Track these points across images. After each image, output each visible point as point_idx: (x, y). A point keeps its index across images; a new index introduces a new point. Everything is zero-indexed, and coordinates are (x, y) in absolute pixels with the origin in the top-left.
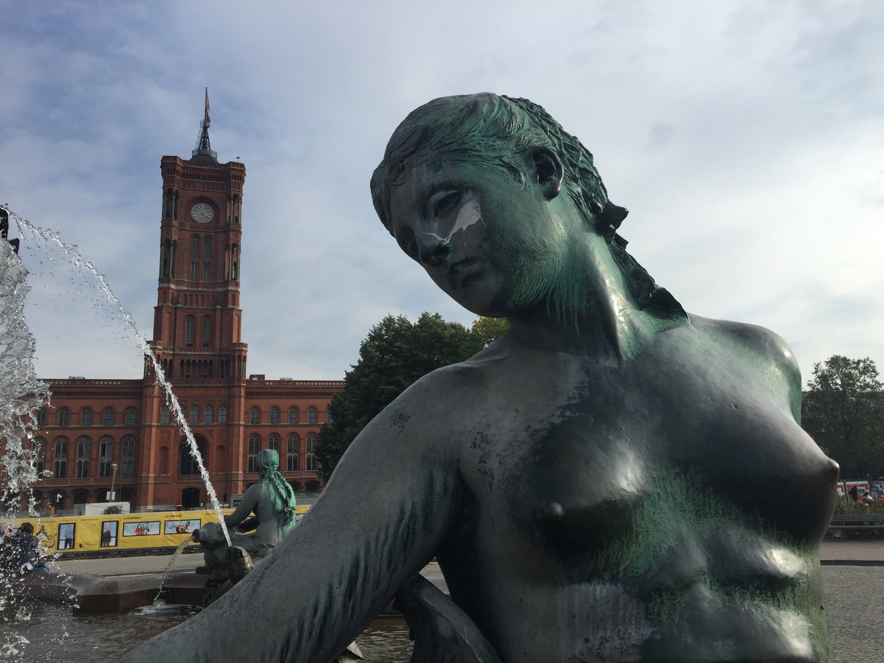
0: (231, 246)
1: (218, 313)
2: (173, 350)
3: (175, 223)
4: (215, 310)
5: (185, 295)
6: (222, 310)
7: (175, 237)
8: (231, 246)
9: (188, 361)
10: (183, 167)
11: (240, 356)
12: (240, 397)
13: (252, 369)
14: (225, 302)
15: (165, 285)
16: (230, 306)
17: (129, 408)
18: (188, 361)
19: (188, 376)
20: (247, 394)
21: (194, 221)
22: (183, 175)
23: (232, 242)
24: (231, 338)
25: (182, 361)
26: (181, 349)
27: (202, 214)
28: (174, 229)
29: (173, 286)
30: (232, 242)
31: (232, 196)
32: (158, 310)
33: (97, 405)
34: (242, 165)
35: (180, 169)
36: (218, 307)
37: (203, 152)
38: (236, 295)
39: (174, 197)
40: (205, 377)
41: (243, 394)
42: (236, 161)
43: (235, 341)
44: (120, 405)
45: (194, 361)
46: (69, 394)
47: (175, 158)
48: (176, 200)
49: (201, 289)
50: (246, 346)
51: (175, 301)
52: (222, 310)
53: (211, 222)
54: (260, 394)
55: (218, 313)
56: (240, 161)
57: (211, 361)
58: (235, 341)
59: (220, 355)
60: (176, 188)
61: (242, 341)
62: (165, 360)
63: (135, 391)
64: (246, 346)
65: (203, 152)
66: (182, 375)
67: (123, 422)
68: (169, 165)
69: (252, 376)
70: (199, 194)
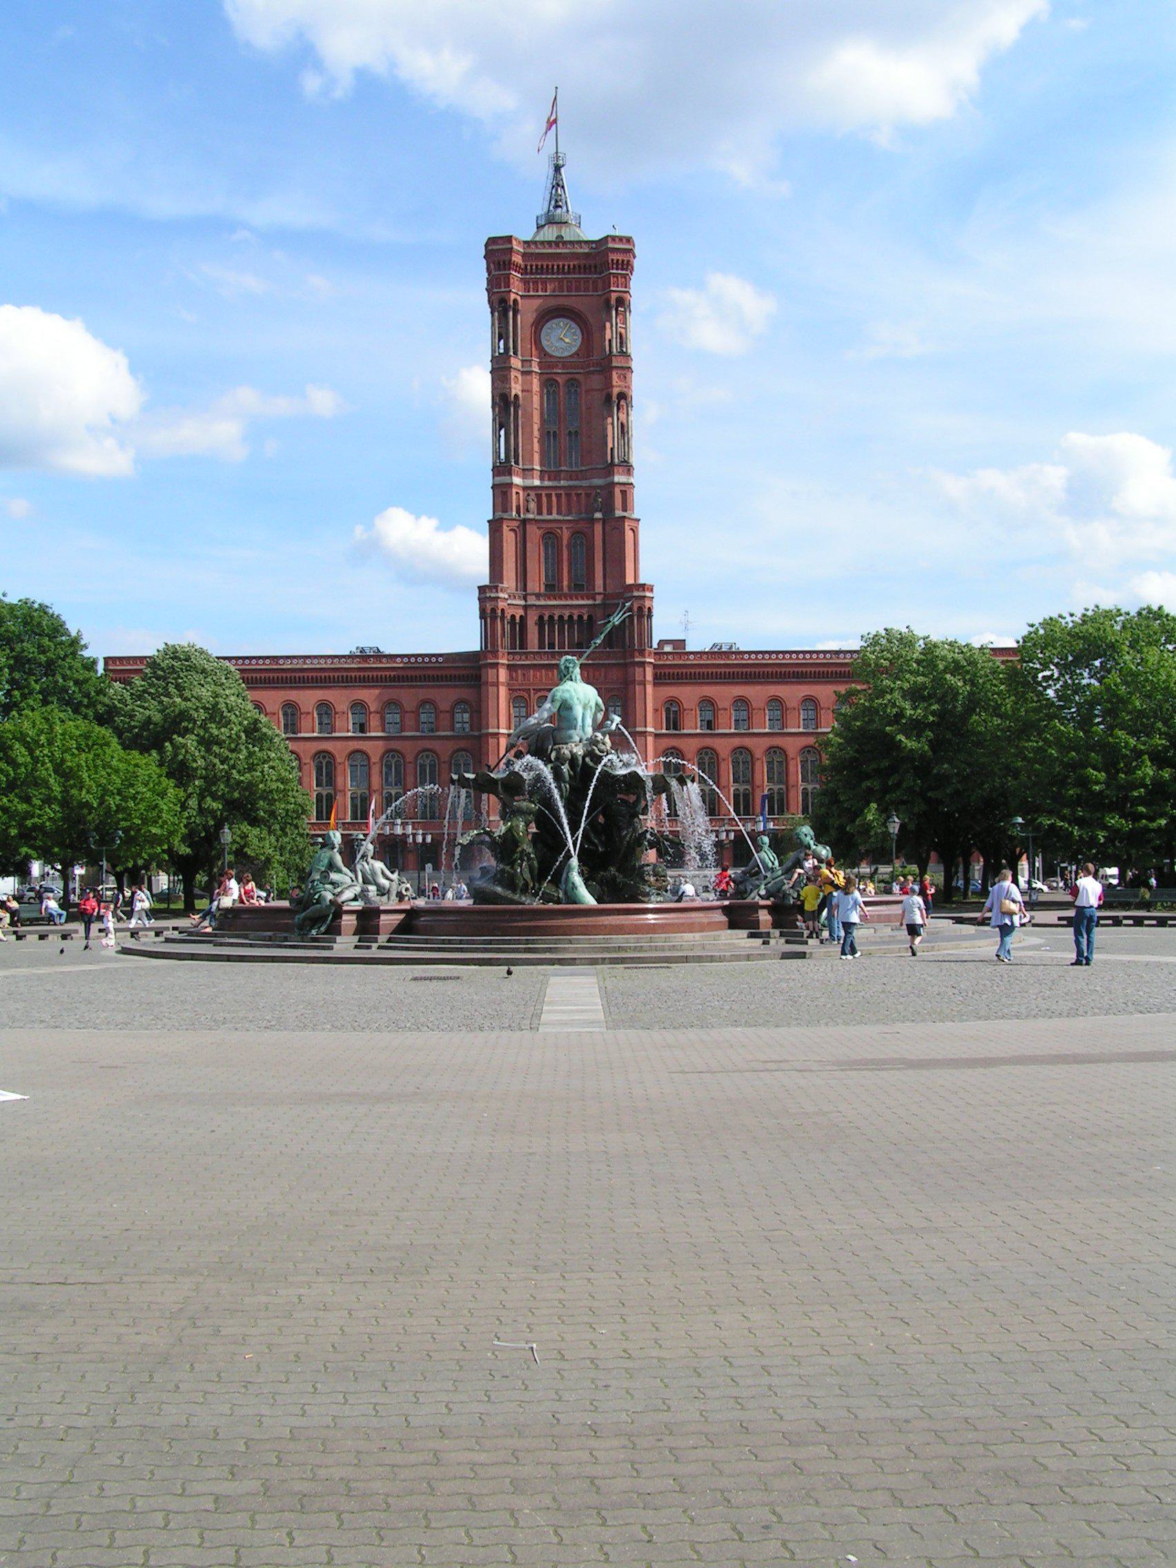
0: (614, 398)
1: (598, 528)
3: (516, 363)
4: (593, 521)
5: (539, 497)
6: (604, 521)
7: (516, 389)
9: (551, 617)
10: (524, 255)
11: (640, 609)
12: (644, 683)
13: (664, 626)
14: (608, 508)
16: (619, 513)
17: (460, 701)
20: (655, 677)
22: (524, 271)
23: (616, 391)
25: (541, 618)
26: (538, 596)
27: (563, 339)
28: (513, 373)
29: (517, 480)
30: (616, 391)
31: (613, 302)
34: (629, 240)
35: (517, 259)
36: (598, 515)
41: (649, 677)
43: (630, 580)
44: (445, 697)
47: (509, 239)
49: (563, 483)
53: (577, 354)
55: (598, 528)
58: (630, 580)
60: (513, 296)
61: (642, 580)
62: (513, 617)
63: (464, 672)
68: (498, 254)
69: (662, 643)
70: (552, 303)
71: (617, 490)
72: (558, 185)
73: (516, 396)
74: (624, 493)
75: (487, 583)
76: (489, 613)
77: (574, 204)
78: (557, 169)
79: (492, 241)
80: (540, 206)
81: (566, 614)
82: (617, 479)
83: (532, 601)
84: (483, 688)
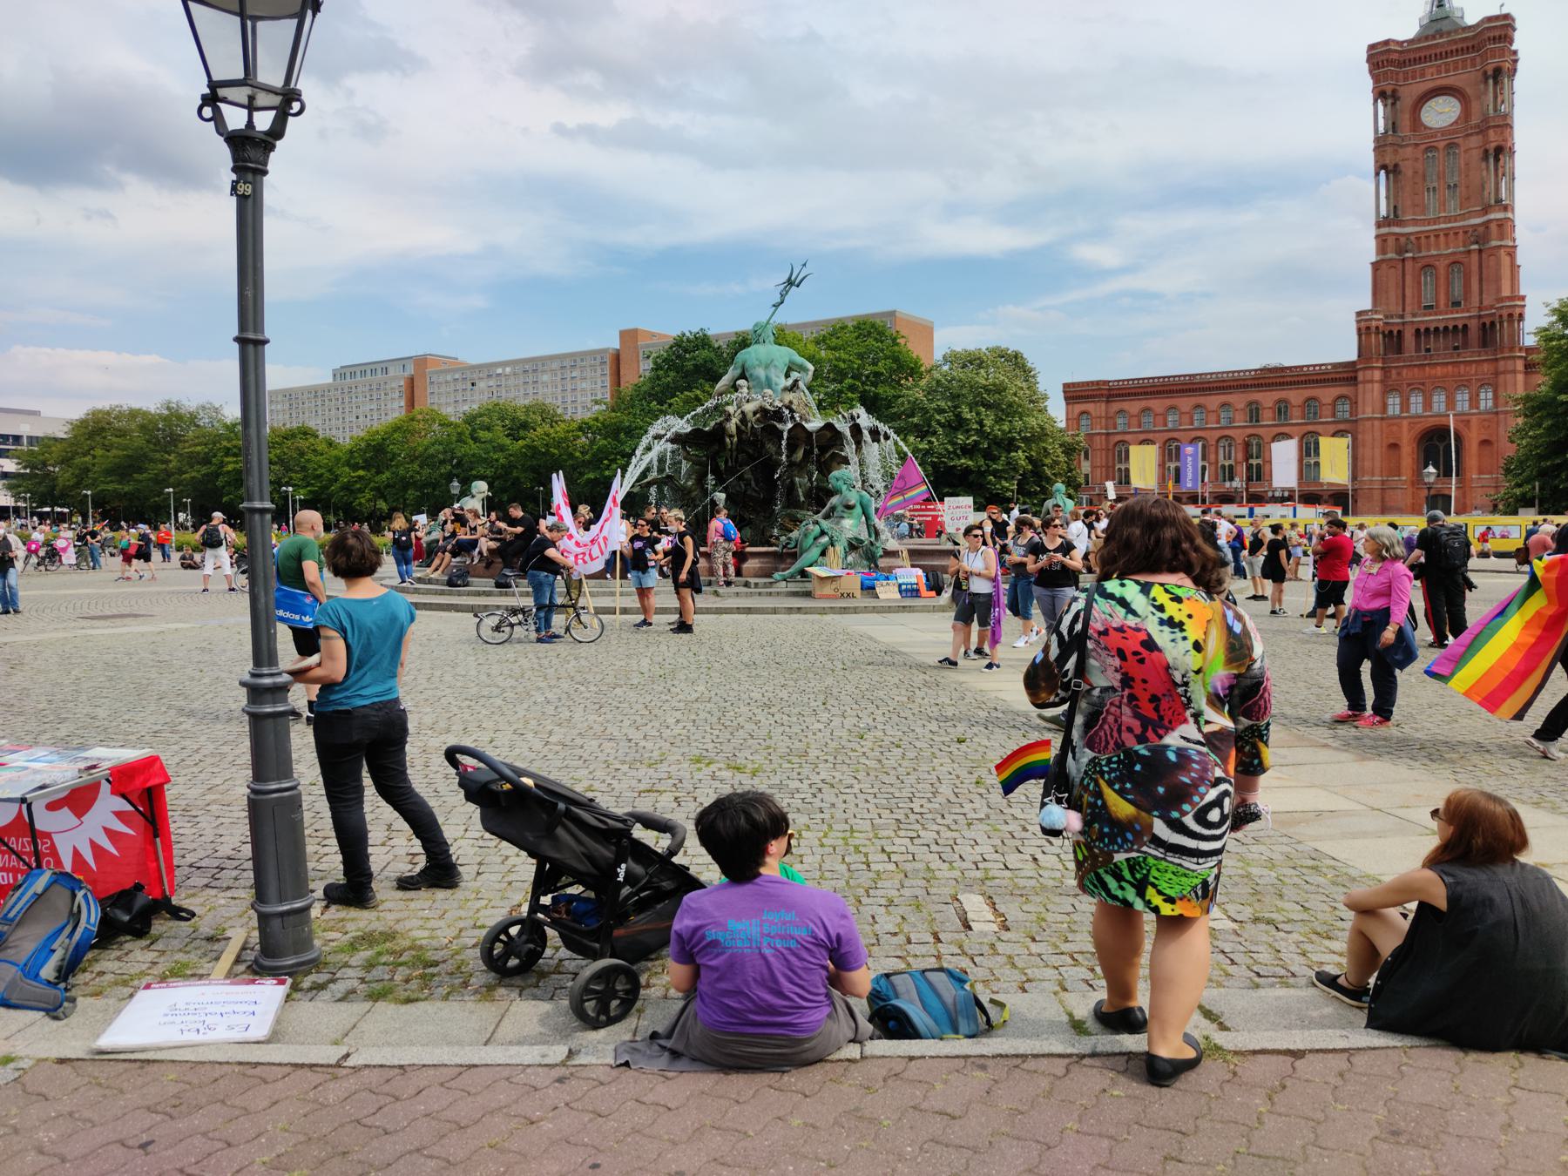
1: (1475, 257)
2: (1402, 317)
8: (1491, 151)
9: (1427, 330)
11: (1510, 315)
15: (1384, 230)
16: (1494, 243)
18: (1427, 330)
19: (1428, 350)
21: (1426, 128)
23: (1493, 145)
24: (1499, 290)
25: (1418, 331)
26: (1414, 315)
27: (1441, 113)
29: (1397, 230)
31: (1490, 73)
33: (1295, 396)
34: (1507, 16)
36: (1475, 247)
38: (1505, 227)
39: (1390, 101)
40: (1456, 348)
42: (1495, 12)
43: (1506, 292)
44: (1327, 394)
45: (1437, 329)
46: (1258, 386)
48: (1393, 104)
50: (1523, 298)
51: (1401, 250)
52: (1480, 251)
53: (1456, 122)
56: (1505, 11)
57: (1465, 326)
58: (1506, 292)
59: (1480, 317)
63: (1345, 375)
66: (1418, 349)
67: (1334, 415)
70: (1431, 85)
71: (1493, 226)
73: (1396, 166)
74: (1500, 226)
76: (1364, 331)
79: (1372, 47)
82: (1492, 216)
83: (1408, 319)
84: (1360, 386)
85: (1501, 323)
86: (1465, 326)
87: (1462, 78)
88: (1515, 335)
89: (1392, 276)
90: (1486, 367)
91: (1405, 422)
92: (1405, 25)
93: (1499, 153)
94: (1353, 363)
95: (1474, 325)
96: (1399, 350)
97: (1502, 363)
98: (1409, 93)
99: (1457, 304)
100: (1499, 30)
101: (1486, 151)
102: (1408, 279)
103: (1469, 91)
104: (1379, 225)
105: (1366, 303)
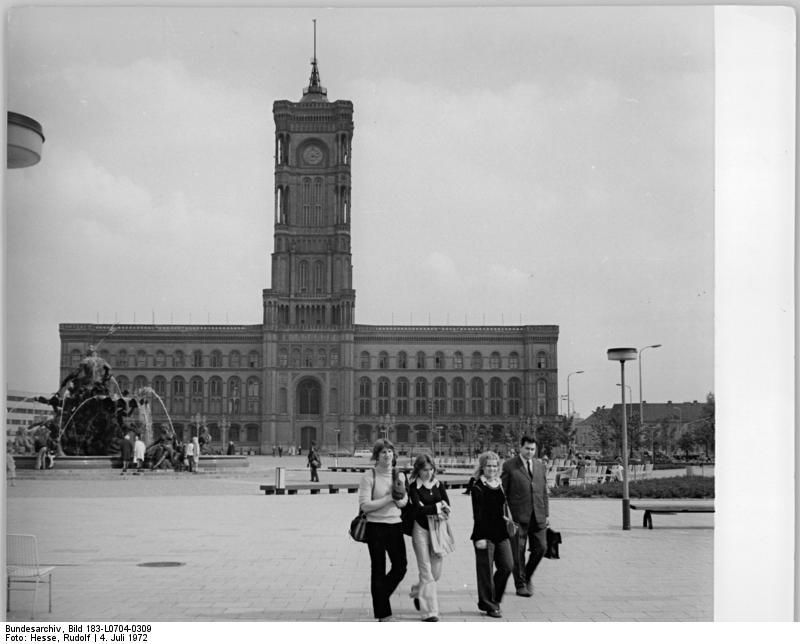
1: (329, 258)
23: (340, 185)
25: (297, 306)
27: (313, 155)
32: (275, 257)
34: (349, 103)
37: (315, 89)
41: (352, 339)
43: (346, 286)
54: (369, 339)
63: (253, 334)
64: (354, 291)
65: (315, 89)
66: (297, 319)
68: (281, 109)
70: (306, 136)
72: (315, 72)
74: (343, 239)
75: (269, 287)
77: (324, 83)
78: (314, 64)
79: (276, 103)
80: (307, 83)
81: (310, 305)
84: (264, 345)
85: (343, 306)
86: (324, 307)
87: (327, 138)
88: (350, 317)
89: (283, 264)
90: (334, 338)
91: (290, 374)
92: (296, 98)
93: (344, 191)
94: (261, 326)
95: (328, 306)
96: (287, 322)
97: (343, 336)
98: (297, 139)
99: (319, 290)
100: (344, 110)
101: (337, 188)
102: (293, 268)
103: (330, 146)
104: (277, 226)
105: (269, 287)
